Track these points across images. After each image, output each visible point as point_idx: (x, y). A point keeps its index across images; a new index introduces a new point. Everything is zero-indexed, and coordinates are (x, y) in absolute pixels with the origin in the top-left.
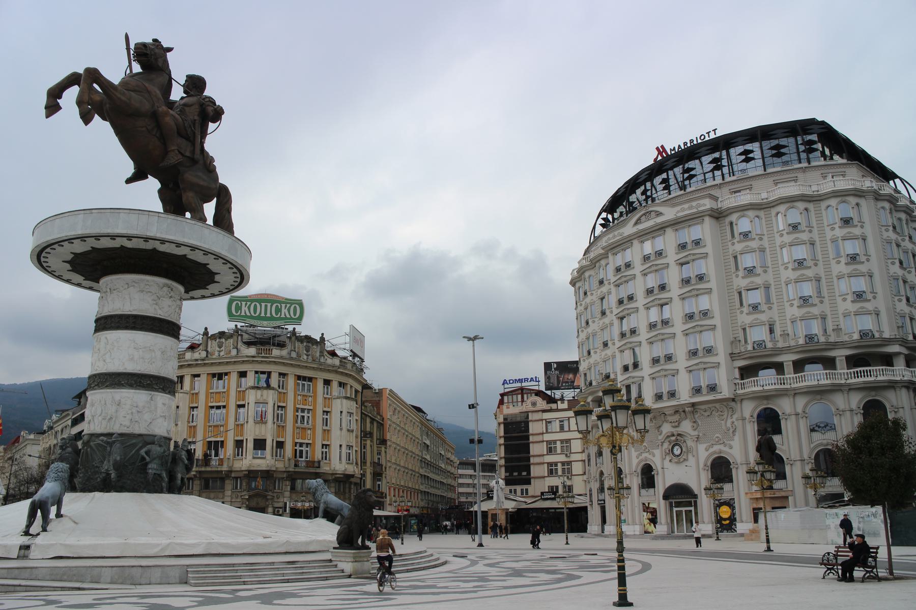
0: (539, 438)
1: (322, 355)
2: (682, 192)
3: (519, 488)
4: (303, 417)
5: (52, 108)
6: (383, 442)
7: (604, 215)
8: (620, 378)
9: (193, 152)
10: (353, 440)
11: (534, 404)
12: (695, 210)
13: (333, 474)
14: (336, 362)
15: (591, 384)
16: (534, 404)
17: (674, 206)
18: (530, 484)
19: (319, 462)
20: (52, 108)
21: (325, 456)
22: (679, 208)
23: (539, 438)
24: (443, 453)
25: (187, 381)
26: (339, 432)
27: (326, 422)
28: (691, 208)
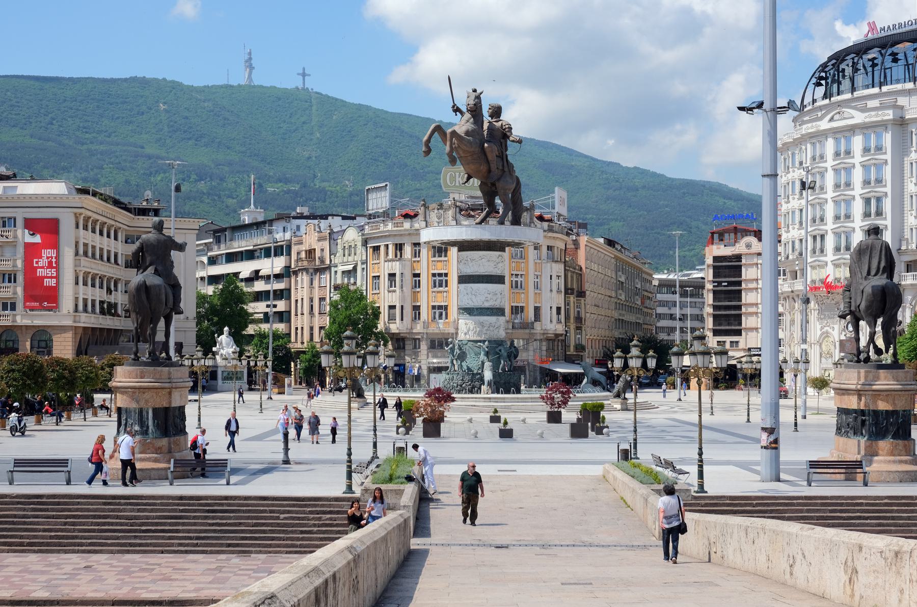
0: (753, 285)
1: (531, 219)
2: (876, 90)
3: (728, 339)
4: (517, 282)
5: (428, 151)
6: (581, 294)
7: (817, 75)
8: (809, 260)
9: (503, 166)
10: (559, 300)
11: (748, 246)
12: (879, 119)
13: (544, 334)
14: (545, 225)
15: (788, 257)
16: (748, 246)
17: (864, 110)
18: (740, 334)
19: (532, 323)
20: (428, 151)
21: (537, 316)
22: (867, 114)
23: (753, 285)
24: (639, 286)
25: (408, 250)
26: (549, 294)
27: (537, 286)
28: (877, 116)
